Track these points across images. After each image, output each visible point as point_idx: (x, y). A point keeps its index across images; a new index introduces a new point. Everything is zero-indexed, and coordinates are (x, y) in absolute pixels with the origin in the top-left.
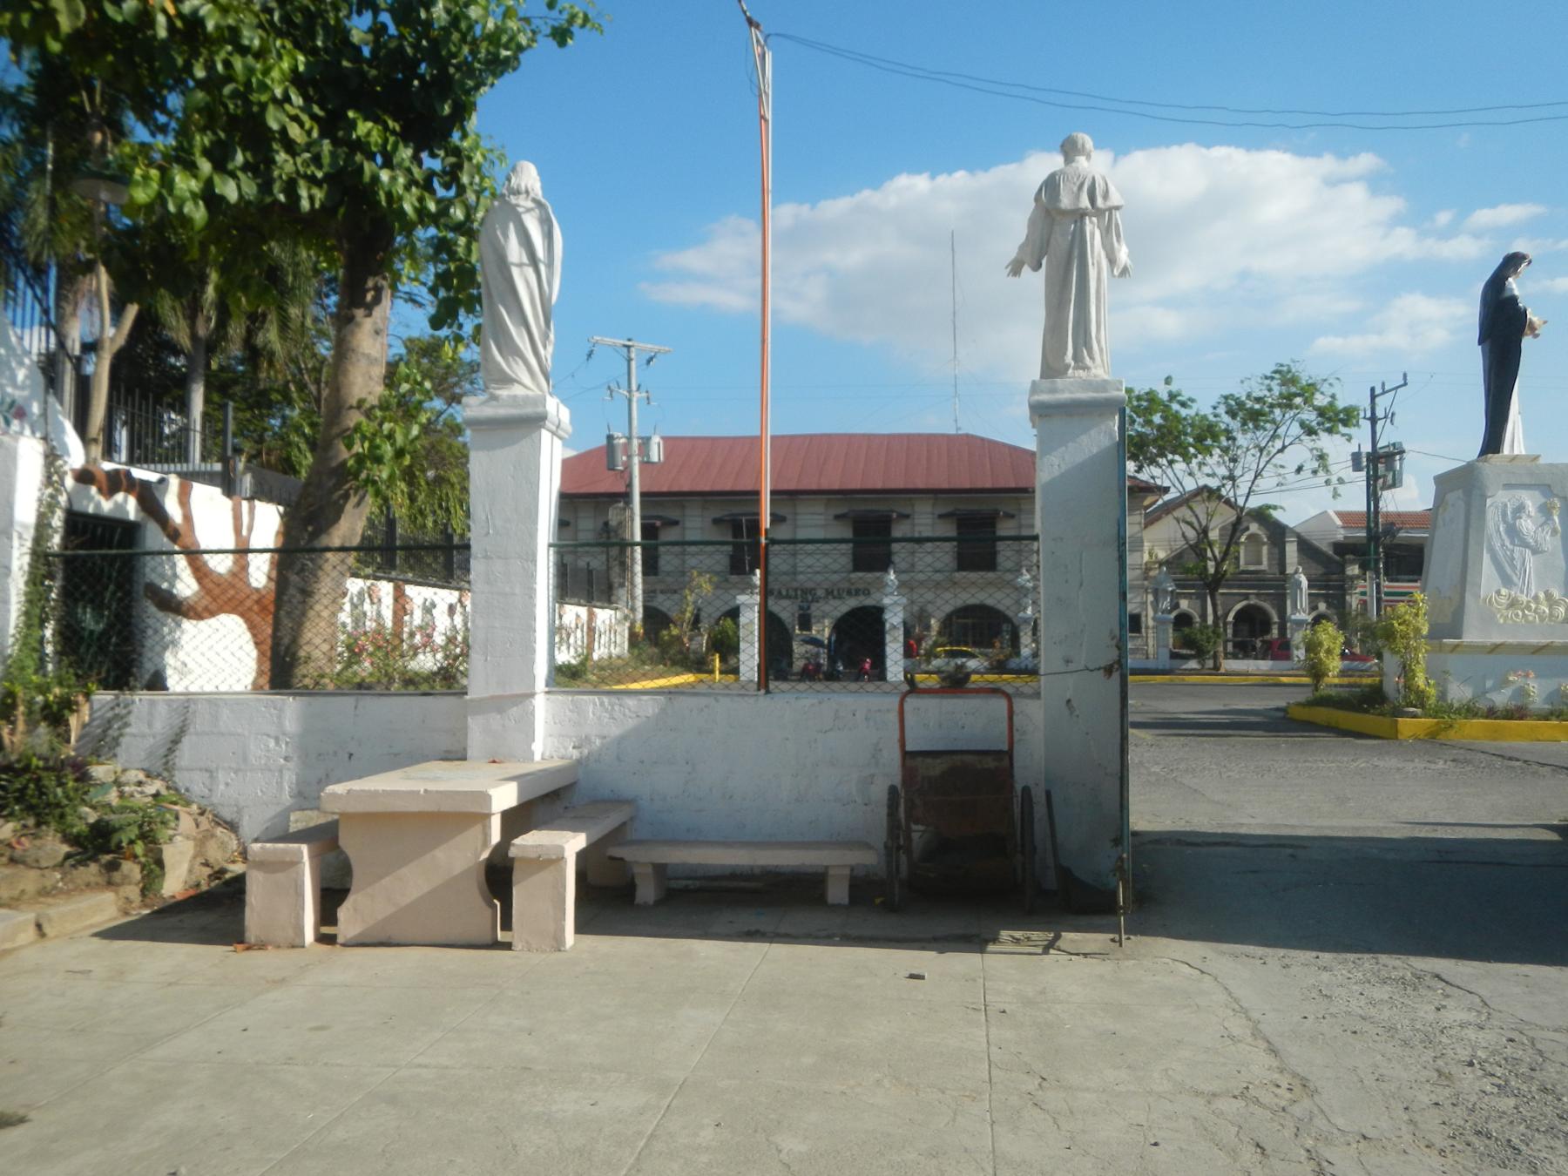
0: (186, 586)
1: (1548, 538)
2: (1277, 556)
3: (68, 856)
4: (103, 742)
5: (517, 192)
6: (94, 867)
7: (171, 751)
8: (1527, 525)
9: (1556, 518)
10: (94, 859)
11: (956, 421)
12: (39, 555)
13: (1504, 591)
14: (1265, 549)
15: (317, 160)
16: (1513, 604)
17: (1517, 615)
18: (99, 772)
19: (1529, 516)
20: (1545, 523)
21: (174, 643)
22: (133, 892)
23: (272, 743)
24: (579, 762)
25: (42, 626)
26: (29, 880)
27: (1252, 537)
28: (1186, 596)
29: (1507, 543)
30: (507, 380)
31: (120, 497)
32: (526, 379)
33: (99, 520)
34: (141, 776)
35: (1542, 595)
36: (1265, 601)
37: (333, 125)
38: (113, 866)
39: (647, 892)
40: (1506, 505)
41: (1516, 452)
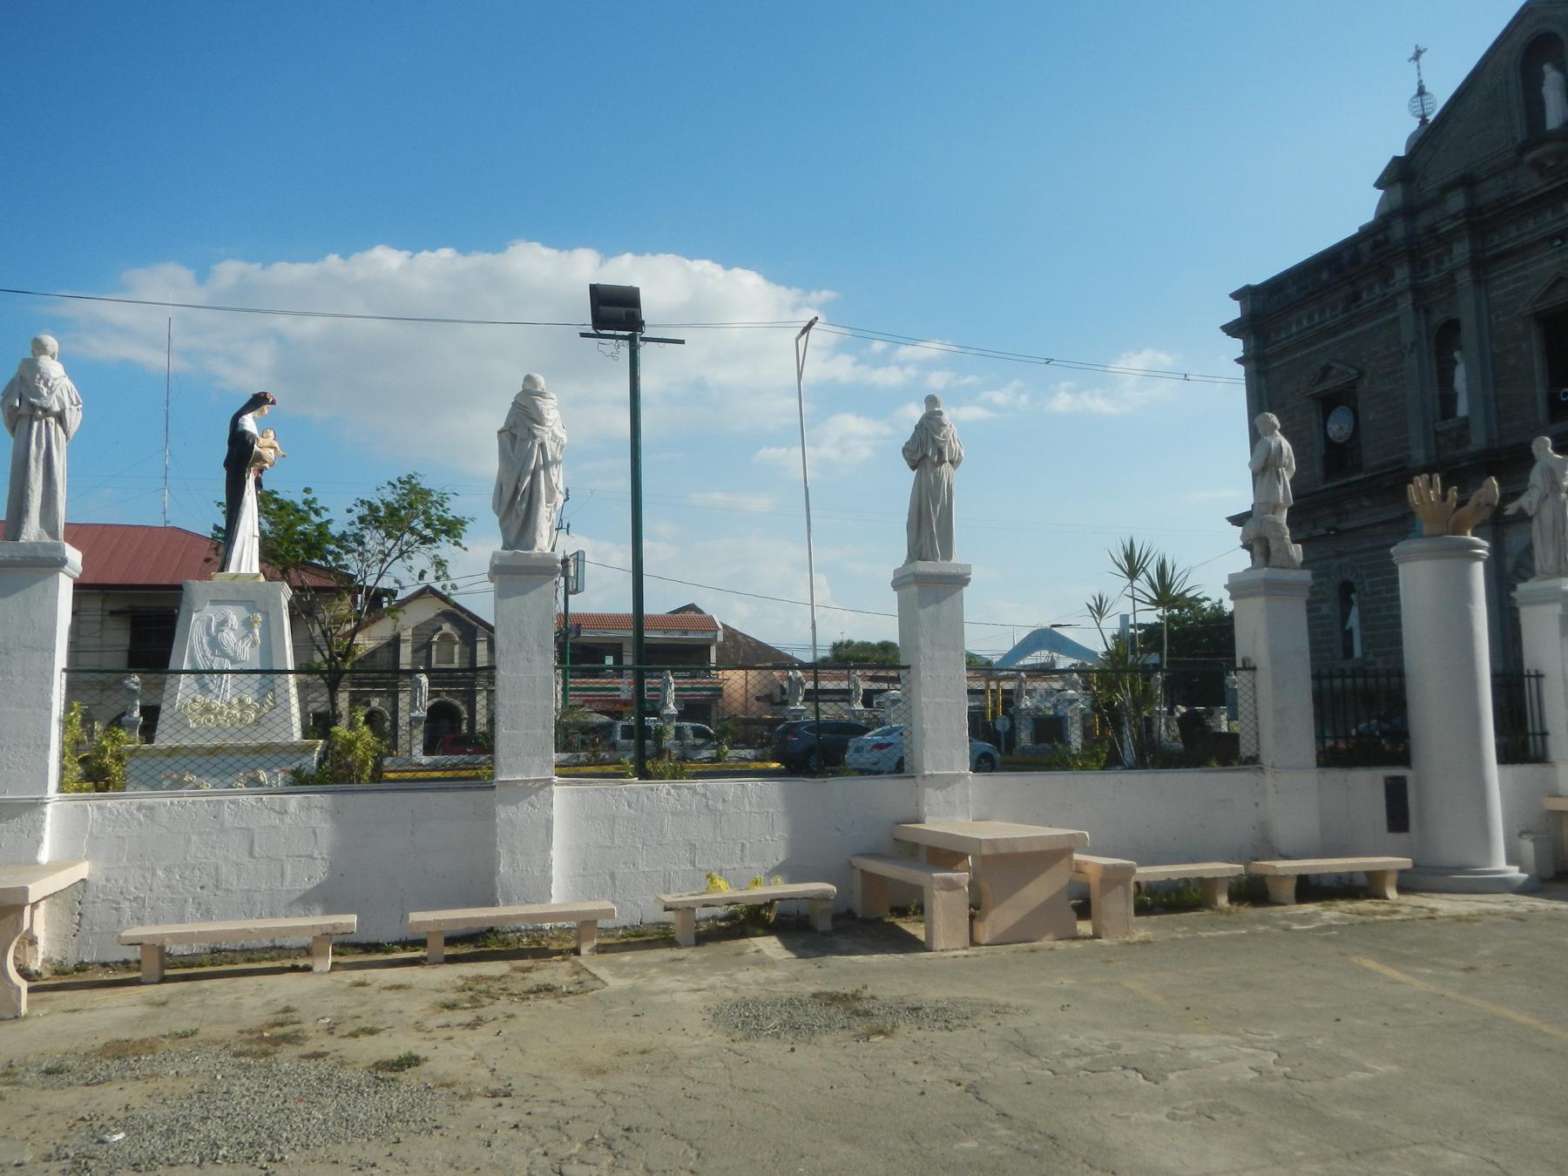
1: (247, 649)
2: (468, 655)
8: (229, 637)
9: (257, 631)
11: (164, 513)
13: (199, 698)
14: (457, 649)
16: (207, 709)
17: (209, 721)
19: (232, 629)
20: (247, 636)
27: (446, 638)
28: (379, 694)
29: (209, 655)
35: (235, 701)
36: (455, 698)
40: (211, 620)
41: (243, 571)
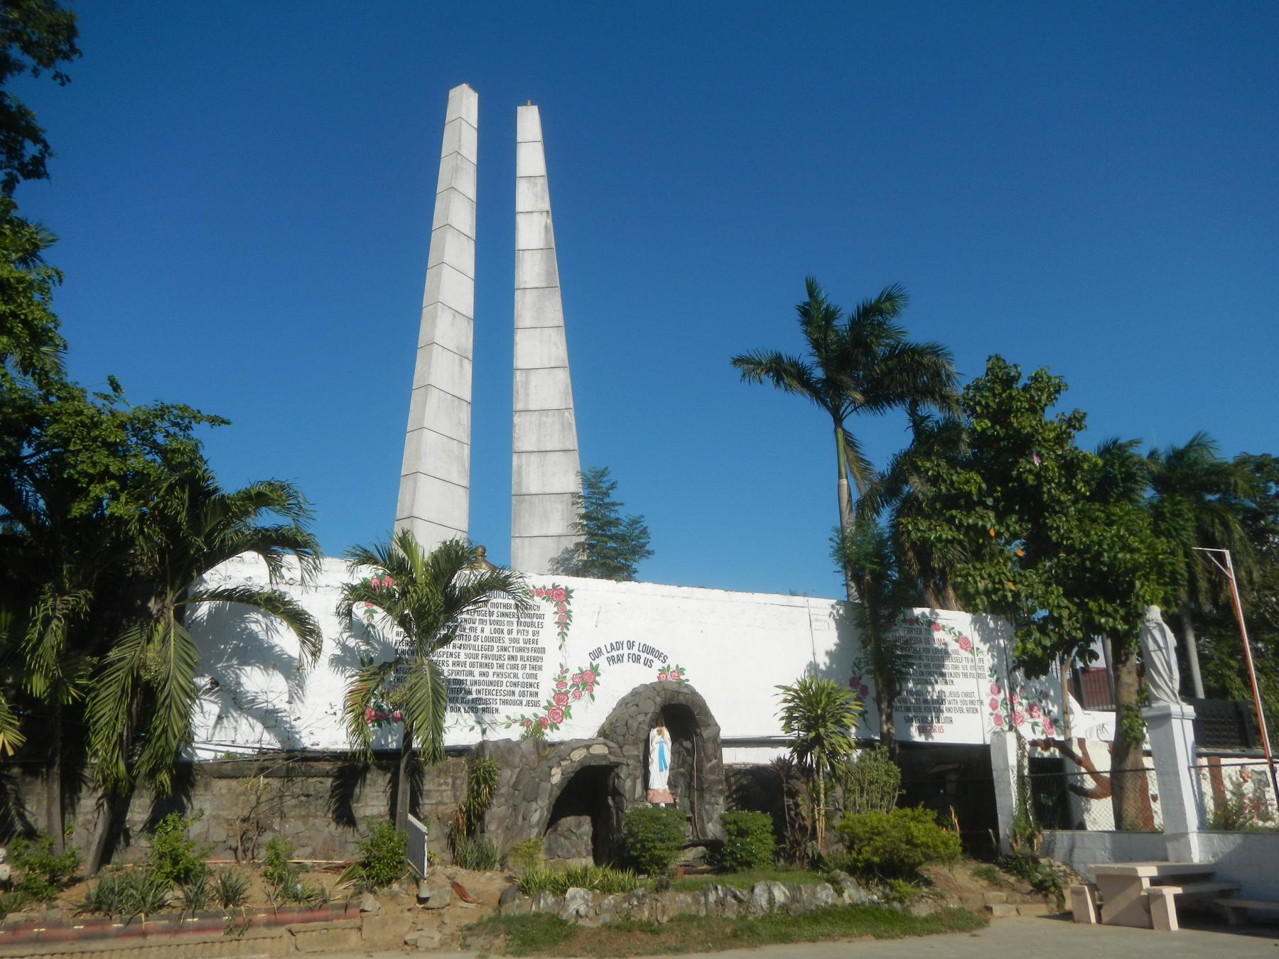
0: (1090, 783)
3: (1032, 891)
4: (1048, 851)
5: (1148, 621)
6: (1040, 895)
7: (1071, 854)
10: (1040, 892)
12: (1021, 777)
15: (1077, 621)
18: (1043, 861)
21: (1088, 810)
22: (1054, 906)
23: (1103, 853)
24: (1216, 864)
25: (1026, 805)
26: (1018, 897)
30: (1157, 699)
31: (1052, 749)
32: (1165, 697)
33: (1043, 760)
34: (1060, 864)
37: (1082, 606)
38: (1046, 896)
39: (1233, 919)
